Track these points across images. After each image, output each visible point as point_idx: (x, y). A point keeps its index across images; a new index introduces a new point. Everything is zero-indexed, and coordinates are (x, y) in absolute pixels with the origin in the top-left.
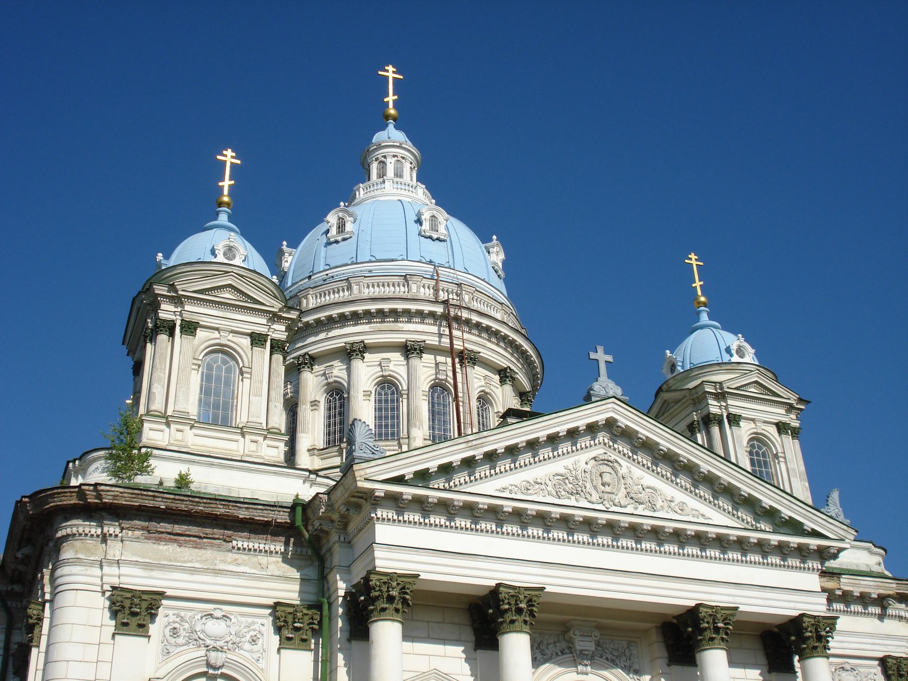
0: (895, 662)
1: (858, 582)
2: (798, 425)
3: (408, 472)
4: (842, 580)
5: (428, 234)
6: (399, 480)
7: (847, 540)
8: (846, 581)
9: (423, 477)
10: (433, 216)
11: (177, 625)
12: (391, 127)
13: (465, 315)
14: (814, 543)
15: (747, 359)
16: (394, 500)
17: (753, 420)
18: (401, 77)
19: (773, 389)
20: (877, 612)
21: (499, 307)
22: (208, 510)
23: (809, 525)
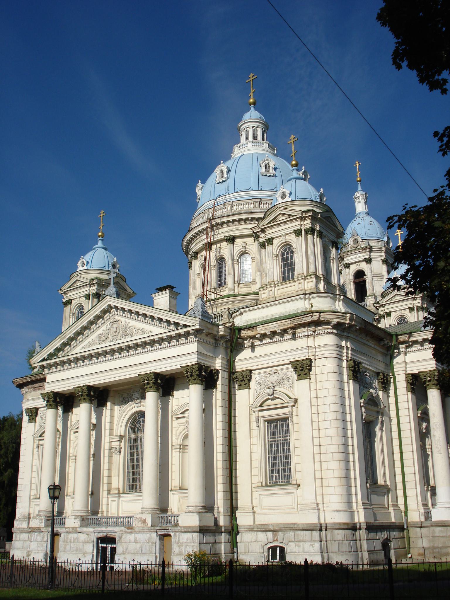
0: (298, 363)
1: (267, 327)
2: (310, 225)
3: (45, 356)
4: (258, 329)
5: (218, 182)
6: (44, 360)
7: (197, 324)
8: (260, 328)
9: (51, 356)
10: (222, 170)
11: (43, 416)
12: (252, 109)
13: (219, 221)
14: (182, 331)
15: (287, 199)
16: (43, 367)
17: (280, 236)
18: (256, 77)
19: (289, 213)
20: (290, 337)
21: (252, 201)
22: (39, 378)
23: (181, 323)
